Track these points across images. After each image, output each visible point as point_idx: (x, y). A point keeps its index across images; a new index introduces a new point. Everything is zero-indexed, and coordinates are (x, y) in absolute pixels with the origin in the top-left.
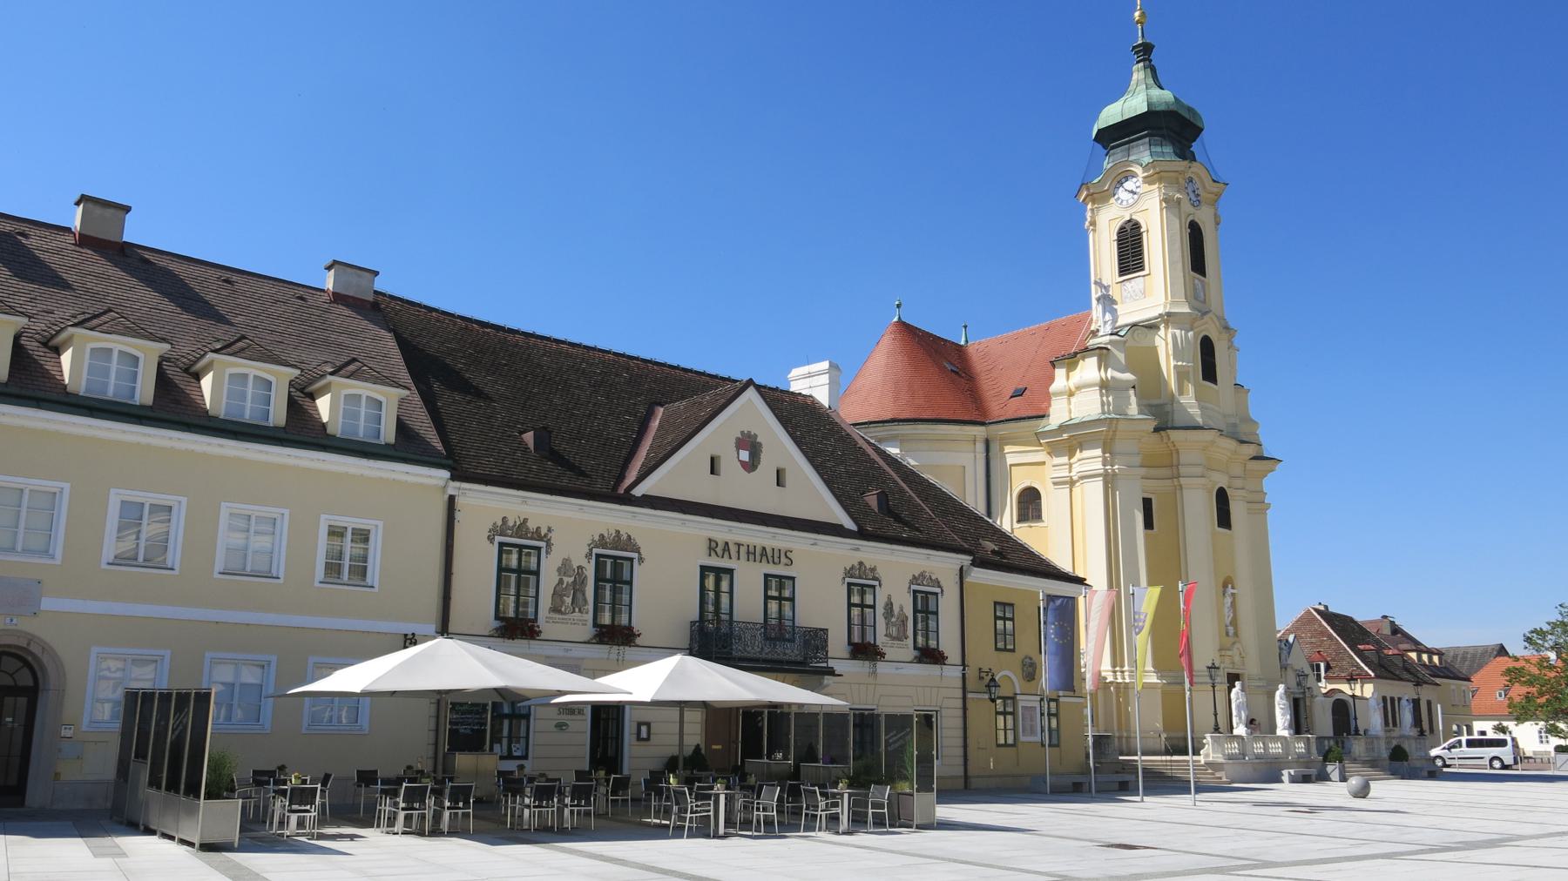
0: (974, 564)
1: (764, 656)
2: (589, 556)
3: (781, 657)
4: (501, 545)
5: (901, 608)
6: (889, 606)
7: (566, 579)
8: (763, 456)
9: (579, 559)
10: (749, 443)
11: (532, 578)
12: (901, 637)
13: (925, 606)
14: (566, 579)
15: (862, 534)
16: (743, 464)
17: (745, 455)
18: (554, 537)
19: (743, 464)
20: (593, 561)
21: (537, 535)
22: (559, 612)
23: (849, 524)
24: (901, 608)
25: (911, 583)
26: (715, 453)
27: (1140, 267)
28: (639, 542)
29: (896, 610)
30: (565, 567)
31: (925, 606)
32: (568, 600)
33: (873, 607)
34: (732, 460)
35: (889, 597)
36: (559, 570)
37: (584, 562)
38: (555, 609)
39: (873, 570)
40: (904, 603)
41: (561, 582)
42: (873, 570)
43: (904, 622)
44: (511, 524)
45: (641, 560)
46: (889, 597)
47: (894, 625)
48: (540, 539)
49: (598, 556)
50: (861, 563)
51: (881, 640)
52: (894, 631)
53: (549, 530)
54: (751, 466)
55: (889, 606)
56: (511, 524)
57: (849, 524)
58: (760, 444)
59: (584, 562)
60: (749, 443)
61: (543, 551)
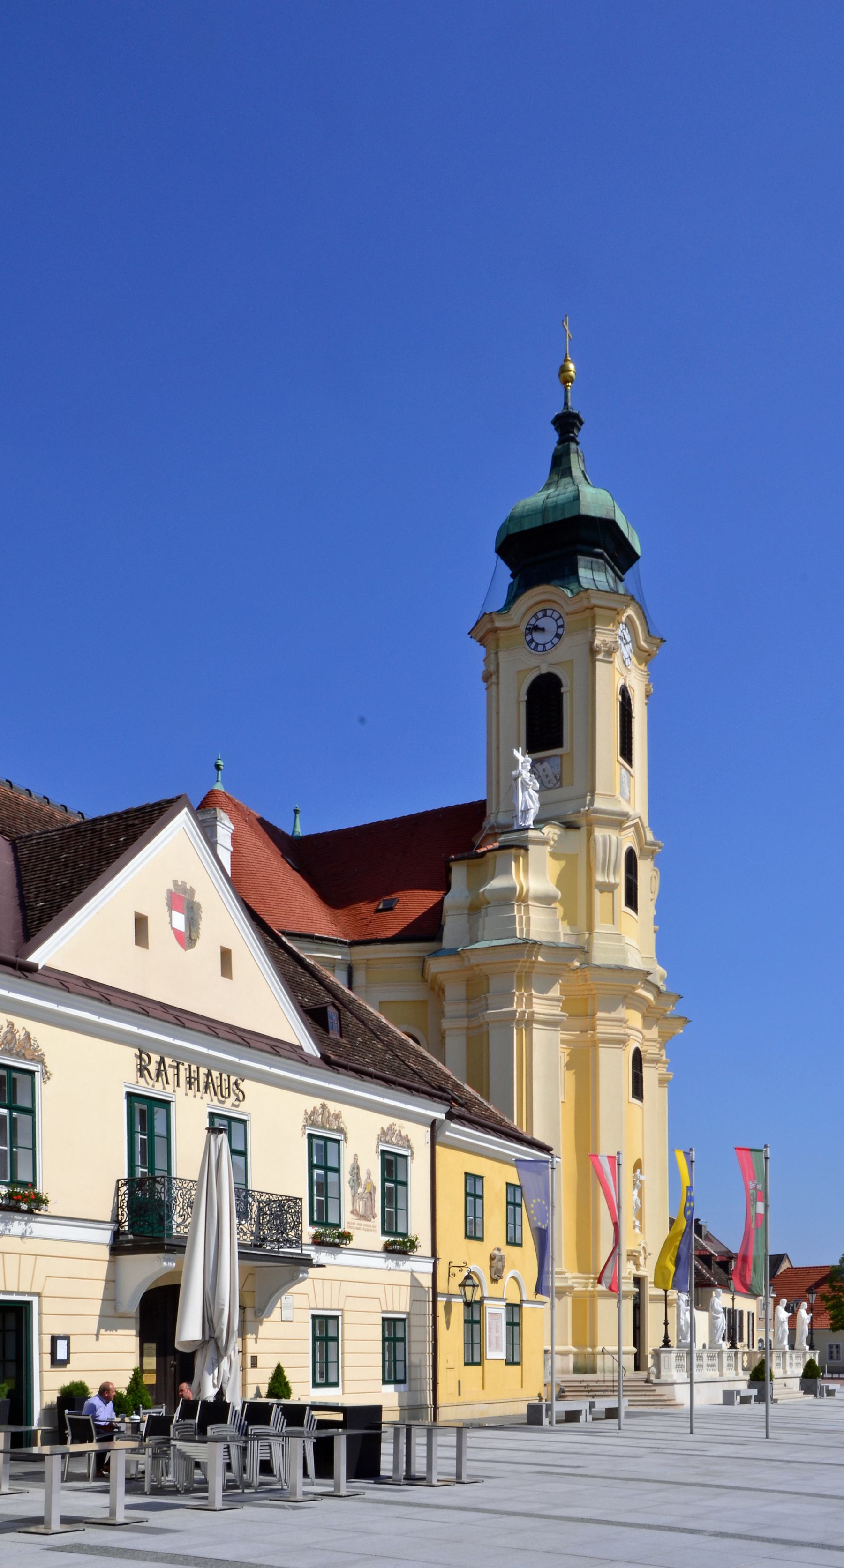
5: (369, 1174)
16: (178, 934)
17: (179, 921)
19: (178, 934)
24: (369, 1174)
27: (557, 742)
33: (337, 1170)
34: (165, 924)
39: (337, 1117)
40: (372, 1169)
42: (337, 1117)
43: (371, 1194)
47: (362, 1198)
50: (324, 1106)
51: (348, 1222)
52: (360, 1206)
60: (182, 900)
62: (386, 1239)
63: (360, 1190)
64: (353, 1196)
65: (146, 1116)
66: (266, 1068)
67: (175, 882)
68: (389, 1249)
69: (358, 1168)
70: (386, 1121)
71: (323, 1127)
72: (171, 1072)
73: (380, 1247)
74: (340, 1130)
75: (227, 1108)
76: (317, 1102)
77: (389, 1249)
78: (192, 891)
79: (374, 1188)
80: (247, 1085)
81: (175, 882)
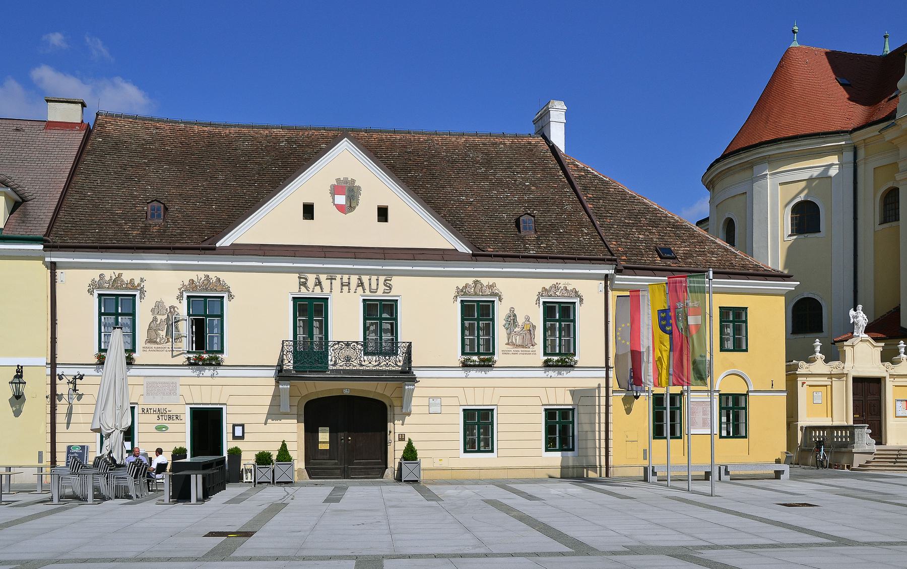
0: (618, 271)
1: (337, 367)
2: (180, 297)
3: (358, 367)
4: (100, 295)
5: (528, 319)
6: (512, 320)
7: (159, 317)
8: (361, 198)
9: (170, 300)
10: (349, 193)
11: (216, 321)
12: (527, 343)
13: (559, 315)
14: (159, 317)
15: (478, 255)
16: (340, 208)
17: (341, 199)
18: (146, 286)
19: (340, 208)
20: (185, 301)
21: (131, 285)
22: (155, 342)
23: (463, 248)
24: (528, 319)
25: (540, 295)
26: (308, 201)
28: (229, 284)
29: (520, 320)
30: (158, 308)
31: (559, 315)
32: (163, 333)
35: (512, 310)
36: (153, 310)
37: (175, 303)
38: (150, 341)
41: (155, 319)
43: (531, 330)
44: (107, 278)
45: (231, 297)
46: (512, 310)
48: (135, 288)
49: (188, 297)
50: (476, 282)
52: (518, 340)
53: (142, 280)
54: (349, 207)
55: (512, 320)
56: (107, 278)
57: (463, 248)
58: (359, 188)
59: (175, 303)
61: (137, 298)
62: (546, 358)
63: (517, 329)
64: (509, 334)
65: (310, 311)
66: (410, 268)
67: (338, 180)
68: (547, 365)
69: (515, 316)
70: (548, 283)
71: (476, 294)
72: (326, 283)
73: (541, 364)
74: (496, 295)
75: (380, 295)
76: (470, 281)
77: (547, 365)
78: (353, 181)
79: (534, 327)
80: (396, 281)
81: (338, 180)
